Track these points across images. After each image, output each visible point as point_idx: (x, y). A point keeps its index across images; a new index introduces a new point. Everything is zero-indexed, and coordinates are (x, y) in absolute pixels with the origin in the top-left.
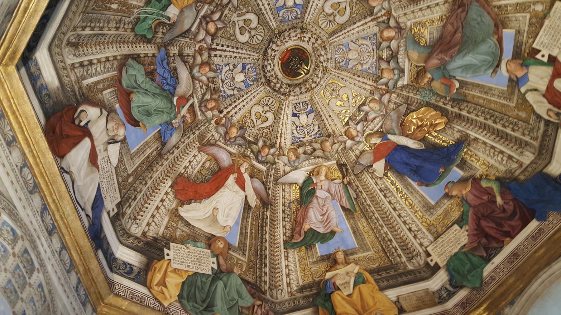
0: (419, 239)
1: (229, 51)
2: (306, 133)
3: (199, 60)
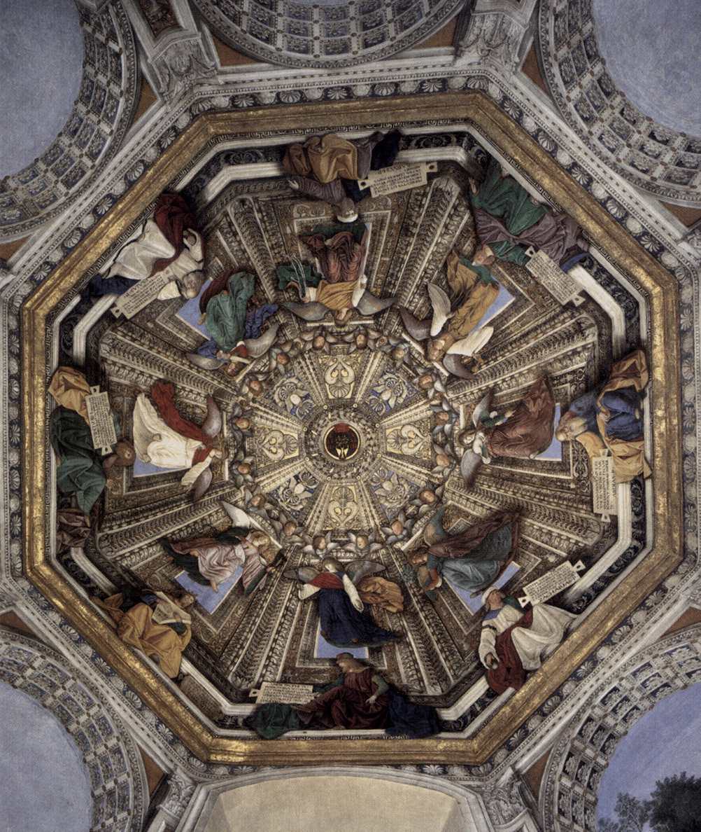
1: (311, 374)
3: (287, 349)
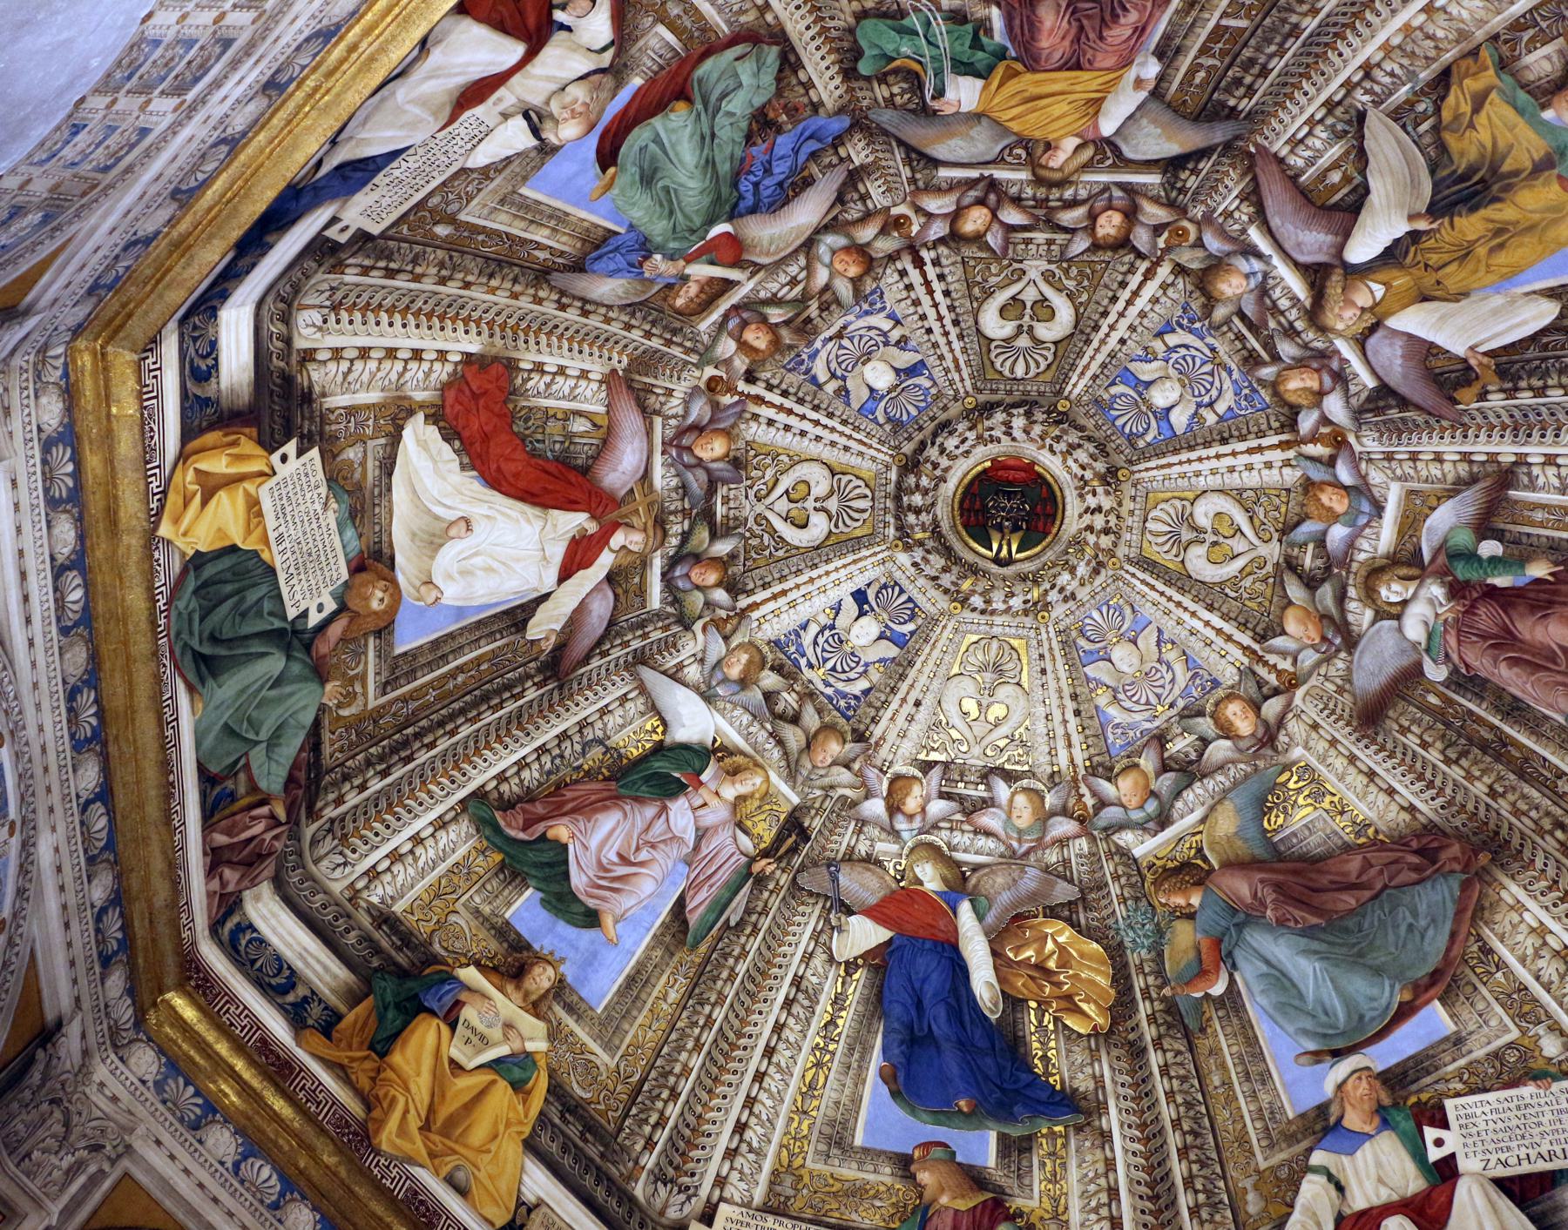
0: (732, 1168)
1: (936, 305)
2: (829, 665)
3: (866, 234)
